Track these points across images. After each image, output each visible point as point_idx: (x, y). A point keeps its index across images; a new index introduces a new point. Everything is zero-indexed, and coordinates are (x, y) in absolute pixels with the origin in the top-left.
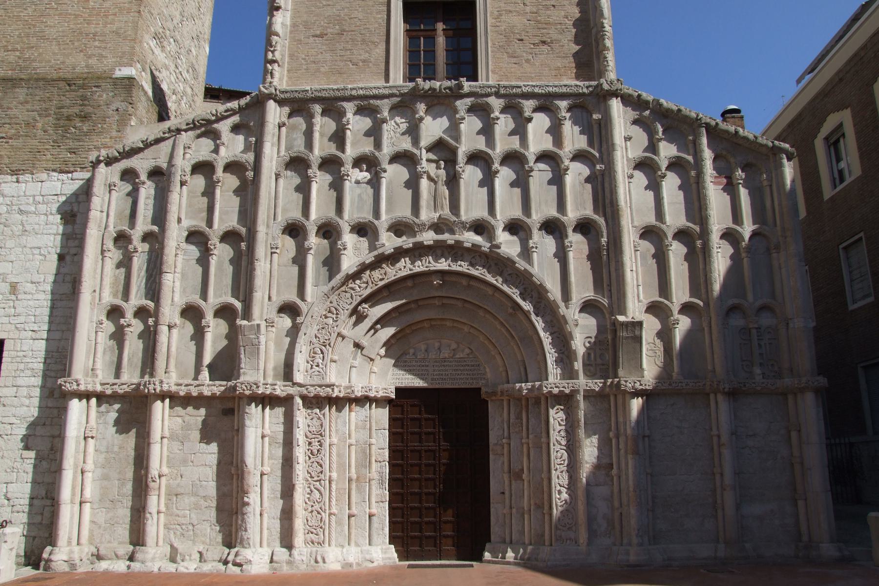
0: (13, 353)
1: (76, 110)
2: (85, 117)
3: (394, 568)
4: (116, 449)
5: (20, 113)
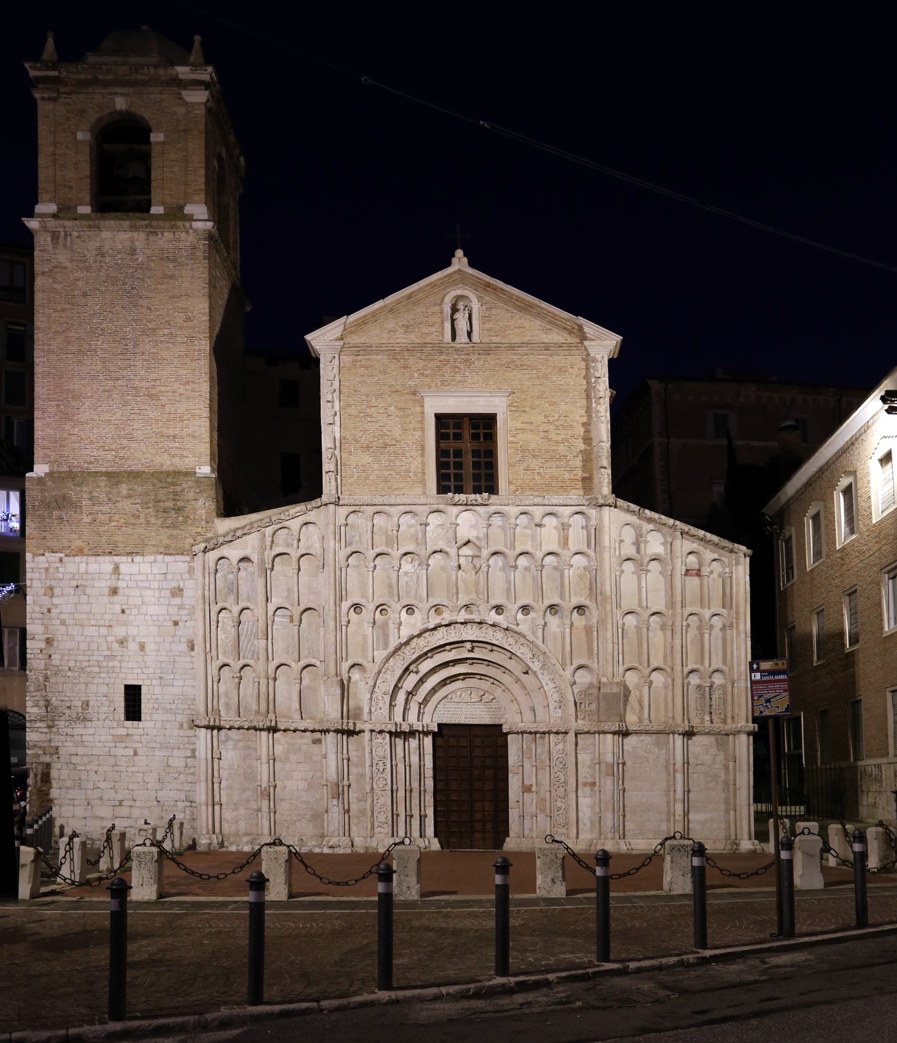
0: (149, 697)
1: (170, 504)
2: (179, 510)
3: (438, 851)
4: (235, 767)
5: (126, 505)
